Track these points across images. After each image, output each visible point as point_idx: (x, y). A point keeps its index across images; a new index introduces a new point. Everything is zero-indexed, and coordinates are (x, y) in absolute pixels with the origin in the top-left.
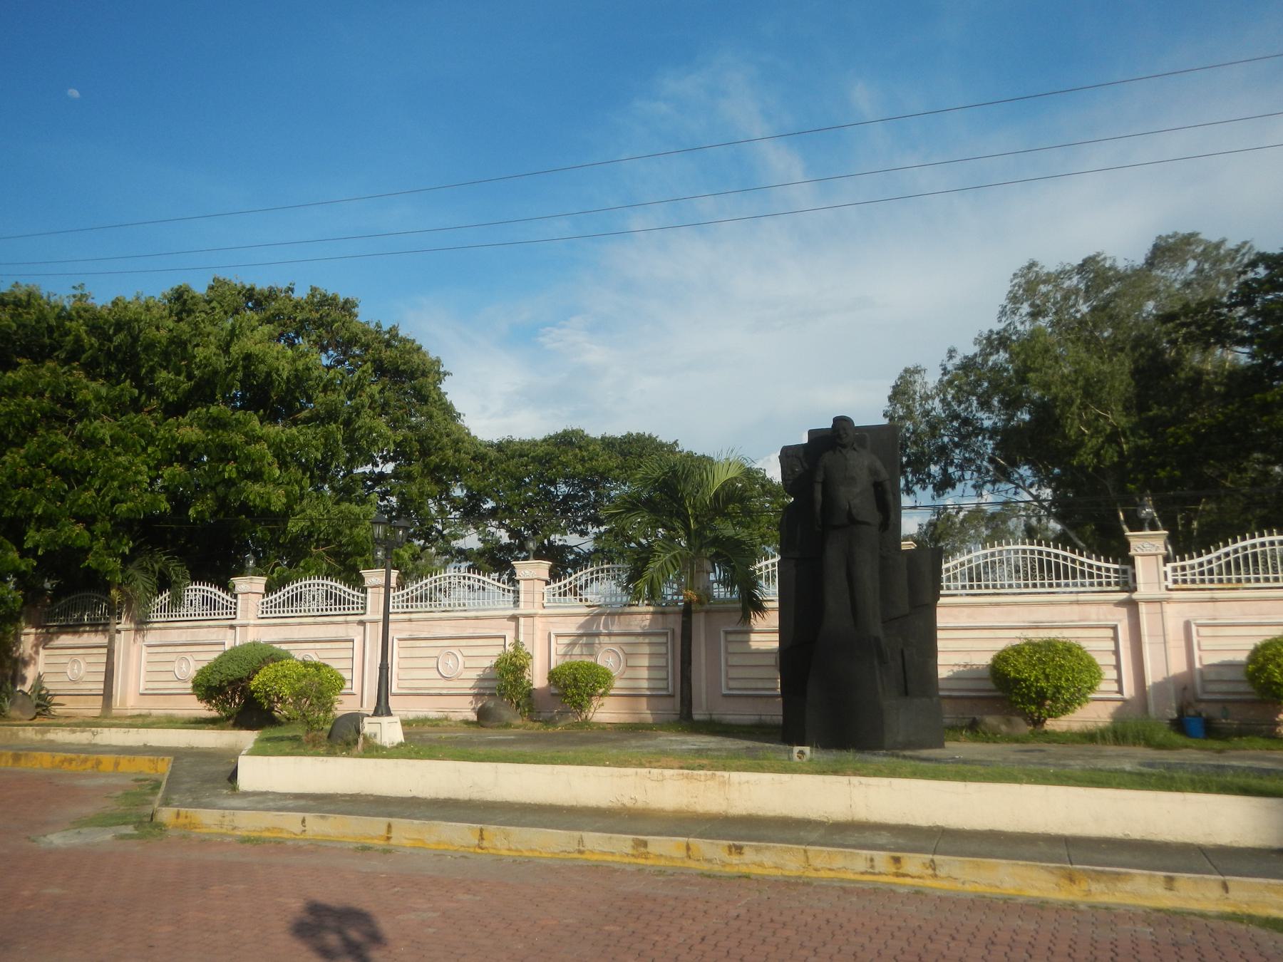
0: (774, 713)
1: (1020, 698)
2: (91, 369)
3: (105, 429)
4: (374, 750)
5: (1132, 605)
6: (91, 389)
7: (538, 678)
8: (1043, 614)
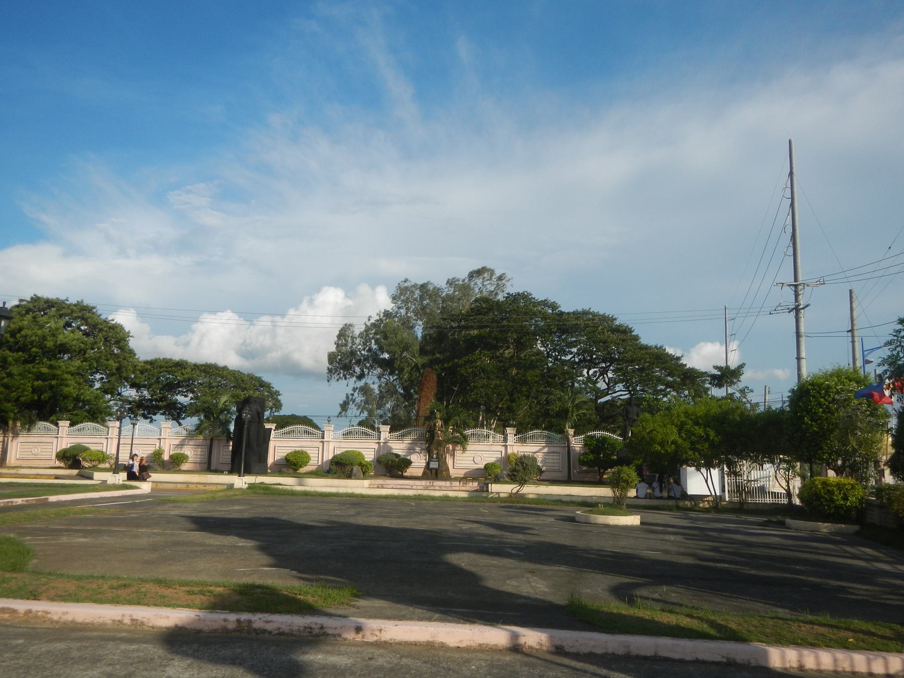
0: (229, 467)
1: (292, 465)
2: (11, 349)
3: (15, 370)
5: (323, 442)
6: (11, 356)
7: (166, 457)
8: (304, 444)
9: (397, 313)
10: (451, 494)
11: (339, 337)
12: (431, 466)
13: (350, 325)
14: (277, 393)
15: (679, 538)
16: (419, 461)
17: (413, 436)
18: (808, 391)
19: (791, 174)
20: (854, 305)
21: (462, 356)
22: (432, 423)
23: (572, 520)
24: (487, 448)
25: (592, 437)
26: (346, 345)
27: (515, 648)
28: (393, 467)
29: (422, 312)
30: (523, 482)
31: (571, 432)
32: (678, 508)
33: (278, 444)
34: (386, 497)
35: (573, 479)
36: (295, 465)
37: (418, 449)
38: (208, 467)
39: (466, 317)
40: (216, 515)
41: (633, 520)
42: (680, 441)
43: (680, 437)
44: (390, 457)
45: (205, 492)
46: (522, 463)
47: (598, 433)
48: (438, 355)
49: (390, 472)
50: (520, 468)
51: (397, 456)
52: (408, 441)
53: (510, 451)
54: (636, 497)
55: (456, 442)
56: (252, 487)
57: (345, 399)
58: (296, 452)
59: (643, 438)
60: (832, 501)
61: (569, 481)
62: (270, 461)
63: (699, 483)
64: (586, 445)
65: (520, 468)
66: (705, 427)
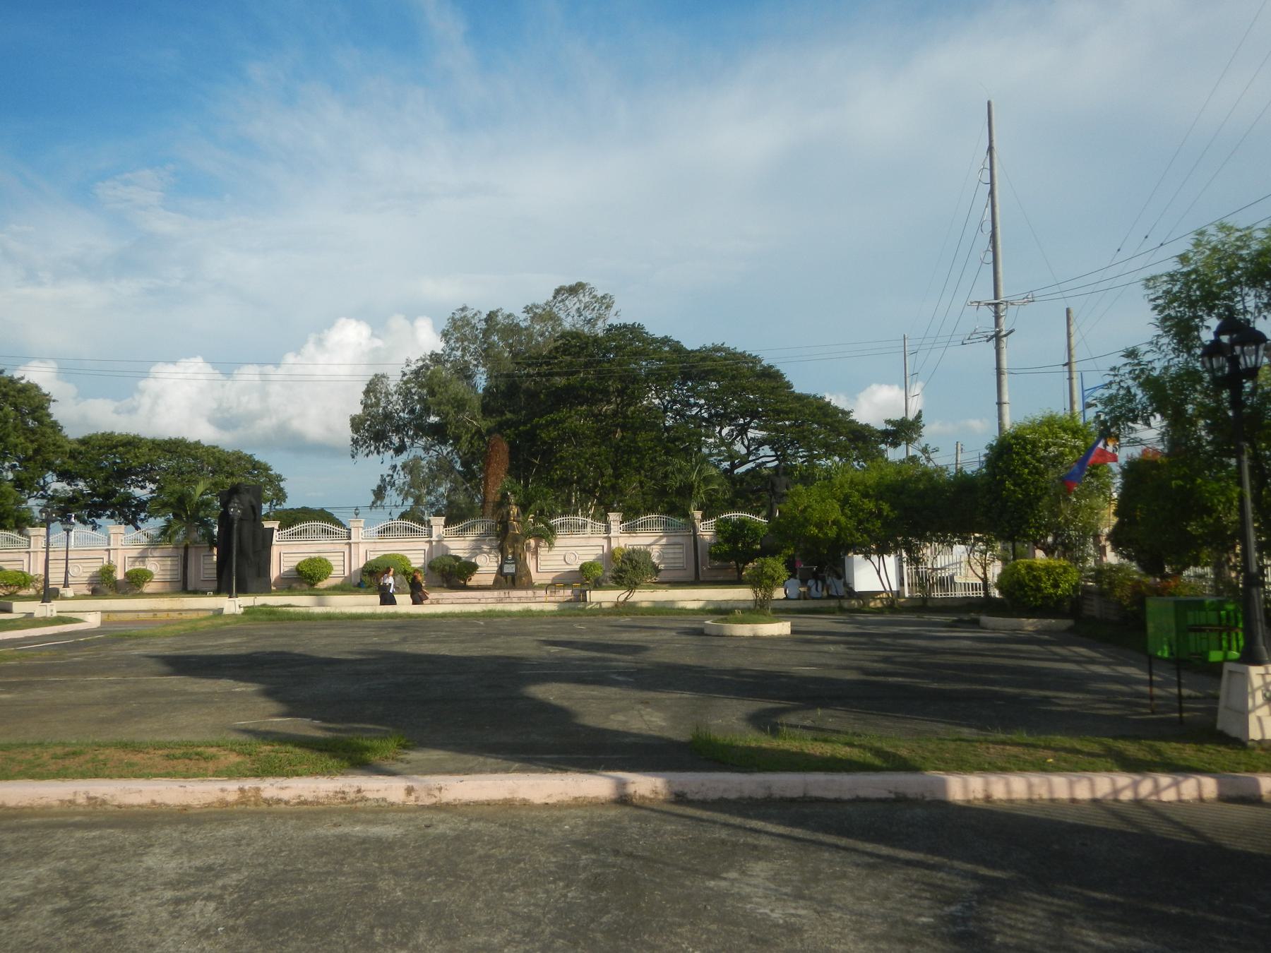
0: (215, 585)
1: (306, 577)
4: (64, 598)
5: (350, 544)
7: (119, 575)
8: (321, 548)
9: (449, 355)
10: (535, 607)
11: (367, 393)
12: (506, 571)
13: (383, 376)
14: (279, 478)
15: (840, 648)
16: (488, 565)
17: (479, 530)
18: (1010, 445)
19: (990, 149)
20: (1072, 329)
21: (542, 415)
22: (504, 511)
23: (700, 632)
24: (583, 542)
25: (726, 521)
26: (377, 404)
27: (623, 800)
28: (453, 574)
29: (487, 354)
30: (632, 586)
31: (698, 515)
32: (842, 610)
33: (284, 550)
34: (444, 616)
35: (701, 579)
36: (311, 578)
37: (486, 548)
38: (184, 586)
39: (549, 359)
40: (200, 652)
41: (782, 628)
42: (843, 519)
43: (844, 514)
44: (447, 561)
45: (181, 622)
46: (631, 560)
47: (734, 516)
48: (509, 416)
49: (448, 581)
50: (628, 567)
51: (457, 558)
52: (470, 537)
53: (614, 544)
54: (787, 598)
55: (539, 536)
56: (249, 611)
57: (379, 482)
58: (312, 560)
59: (794, 518)
60: (1039, 589)
61: (697, 581)
62: (274, 573)
63: (871, 575)
64: (718, 532)
65: (628, 567)
66: (877, 500)
